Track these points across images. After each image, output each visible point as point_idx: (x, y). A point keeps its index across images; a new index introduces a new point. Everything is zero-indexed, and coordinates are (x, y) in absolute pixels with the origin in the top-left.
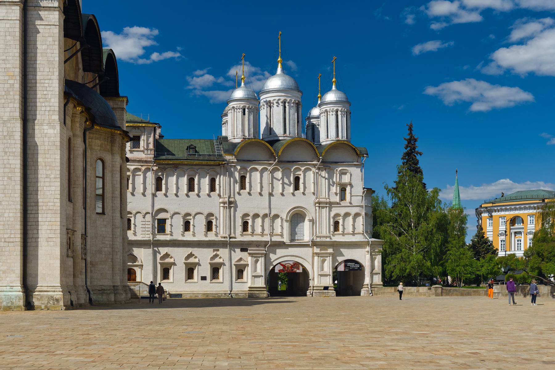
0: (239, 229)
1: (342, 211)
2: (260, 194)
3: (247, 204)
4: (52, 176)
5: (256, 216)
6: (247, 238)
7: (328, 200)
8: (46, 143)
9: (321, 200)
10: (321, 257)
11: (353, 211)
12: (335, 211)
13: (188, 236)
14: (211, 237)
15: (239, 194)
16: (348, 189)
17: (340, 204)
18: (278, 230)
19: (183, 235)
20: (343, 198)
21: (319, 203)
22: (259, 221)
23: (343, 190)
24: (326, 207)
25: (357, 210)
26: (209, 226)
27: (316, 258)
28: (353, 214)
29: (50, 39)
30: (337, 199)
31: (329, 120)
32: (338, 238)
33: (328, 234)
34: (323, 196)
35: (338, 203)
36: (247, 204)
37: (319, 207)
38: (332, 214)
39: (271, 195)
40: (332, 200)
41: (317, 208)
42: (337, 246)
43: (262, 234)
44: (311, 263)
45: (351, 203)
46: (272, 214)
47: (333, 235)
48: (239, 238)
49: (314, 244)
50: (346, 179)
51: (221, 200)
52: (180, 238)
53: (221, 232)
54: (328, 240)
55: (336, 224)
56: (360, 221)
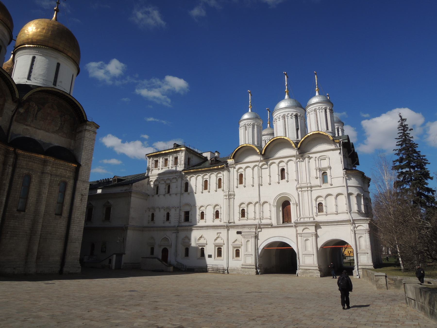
0: (237, 215)
2: (253, 186)
3: (244, 194)
5: (250, 203)
6: (244, 222)
7: (309, 185)
9: (303, 185)
10: (304, 237)
11: (334, 192)
12: (315, 193)
14: (217, 222)
15: (237, 187)
16: (328, 172)
17: (321, 187)
18: (267, 214)
21: (301, 188)
22: (251, 207)
25: (339, 190)
26: (217, 215)
27: (299, 238)
28: (335, 194)
30: (318, 182)
31: (317, 119)
32: (320, 218)
33: (311, 216)
34: (304, 180)
36: (244, 194)
37: (302, 191)
38: (314, 197)
39: (260, 185)
40: (312, 185)
41: (300, 193)
42: (317, 226)
43: (255, 219)
44: (296, 243)
45: (332, 185)
46: (262, 201)
47: (317, 216)
48: (237, 222)
49: (297, 224)
50: (324, 164)
51: (225, 194)
53: (224, 219)
54: (312, 220)
55: (320, 204)
56: (343, 200)
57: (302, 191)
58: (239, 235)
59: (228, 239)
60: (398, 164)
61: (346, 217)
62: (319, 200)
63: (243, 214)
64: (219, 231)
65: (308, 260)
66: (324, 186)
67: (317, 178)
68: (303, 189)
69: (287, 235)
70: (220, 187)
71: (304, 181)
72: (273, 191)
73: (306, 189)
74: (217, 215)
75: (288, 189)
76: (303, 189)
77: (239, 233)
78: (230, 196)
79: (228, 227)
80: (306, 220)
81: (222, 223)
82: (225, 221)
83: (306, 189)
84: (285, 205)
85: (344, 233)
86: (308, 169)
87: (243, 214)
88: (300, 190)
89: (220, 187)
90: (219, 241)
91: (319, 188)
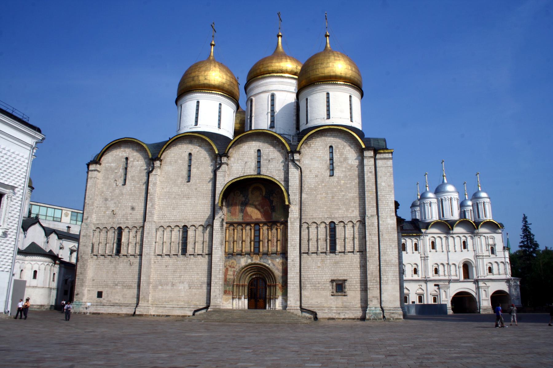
1: (492, 261)
4: (393, 246)
6: (436, 277)
8: (389, 228)
9: (480, 254)
11: (499, 260)
14: (415, 277)
15: (430, 251)
26: (416, 271)
29: (389, 174)
32: (490, 276)
36: (435, 258)
39: (448, 251)
48: (432, 278)
58: (437, 287)
59: (427, 290)
60: (522, 244)
61: (504, 277)
62: (490, 265)
63: (436, 271)
64: (420, 283)
65: (485, 303)
66: (492, 256)
69: (469, 287)
70: (416, 249)
71: (480, 252)
72: (459, 257)
74: (416, 271)
75: (469, 255)
77: (435, 285)
78: (425, 258)
79: (426, 281)
80: (483, 278)
81: (420, 278)
82: (423, 276)
85: (504, 287)
87: (436, 271)
89: (416, 249)
90: (420, 291)
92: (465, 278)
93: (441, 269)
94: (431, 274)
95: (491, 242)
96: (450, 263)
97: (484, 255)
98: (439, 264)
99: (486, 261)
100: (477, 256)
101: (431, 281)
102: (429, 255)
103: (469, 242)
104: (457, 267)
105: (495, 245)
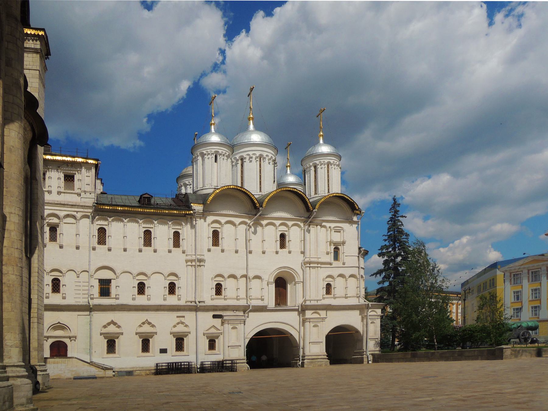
5: (233, 276)
9: (312, 260)
13: (141, 300)
19: (134, 299)
20: (336, 258)
21: (310, 263)
23: (336, 250)
24: (318, 267)
26: (172, 288)
30: (330, 258)
35: (331, 264)
37: (310, 267)
45: (344, 264)
46: (251, 275)
52: (131, 303)
57: (310, 267)
63: (219, 289)
66: (335, 263)
67: (328, 253)
68: (311, 265)
73: (316, 265)
74: (172, 288)
75: (290, 260)
76: (311, 265)
83: (316, 265)
84: (281, 283)
86: (319, 238)
87: (219, 289)
88: (308, 265)
91: (329, 266)
92: (277, 303)
93: (229, 285)
94: (208, 296)
95: (337, 237)
96: (251, 275)
97: (320, 260)
98: (226, 276)
99: (324, 272)
100: (307, 264)
101: (207, 309)
102: (205, 258)
103: (295, 234)
104: (265, 283)
105: (344, 243)
